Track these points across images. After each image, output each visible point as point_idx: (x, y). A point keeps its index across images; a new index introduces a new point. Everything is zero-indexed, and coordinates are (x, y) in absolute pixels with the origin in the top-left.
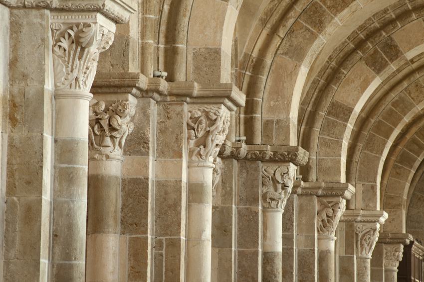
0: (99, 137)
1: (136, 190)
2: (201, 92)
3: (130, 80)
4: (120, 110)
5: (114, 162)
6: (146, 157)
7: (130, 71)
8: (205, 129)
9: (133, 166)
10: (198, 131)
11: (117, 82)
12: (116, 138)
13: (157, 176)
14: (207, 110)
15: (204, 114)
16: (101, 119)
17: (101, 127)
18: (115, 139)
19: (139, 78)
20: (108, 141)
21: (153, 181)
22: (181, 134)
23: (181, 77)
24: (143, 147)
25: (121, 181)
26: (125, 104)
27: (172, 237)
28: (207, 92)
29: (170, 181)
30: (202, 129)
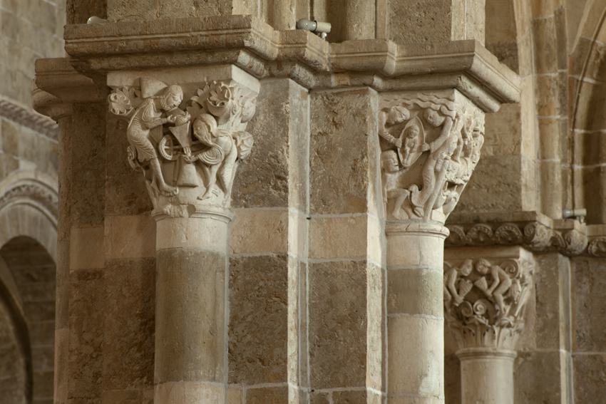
0: (172, 165)
1: (261, 284)
2: (407, 64)
3: (231, 31)
4: (215, 103)
5: (209, 221)
6: (280, 208)
7: (234, 12)
9: (252, 231)
10: (404, 152)
11: (202, 38)
12: (210, 166)
13: (313, 254)
14: (421, 104)
15: (416, 113)
16: (173, 125)
17: (175, 142)
18: (207, 169)
19: (250, 27)
20: (191, 173)
21: (303, 264)
22: (363, 157)
23: (362, 29)
24: (276, 187)
25: (227, 264)
26: (224, 88)
27: (349, 389)
28: (421, 63)
29: (341, 263)
30: (412, 148)
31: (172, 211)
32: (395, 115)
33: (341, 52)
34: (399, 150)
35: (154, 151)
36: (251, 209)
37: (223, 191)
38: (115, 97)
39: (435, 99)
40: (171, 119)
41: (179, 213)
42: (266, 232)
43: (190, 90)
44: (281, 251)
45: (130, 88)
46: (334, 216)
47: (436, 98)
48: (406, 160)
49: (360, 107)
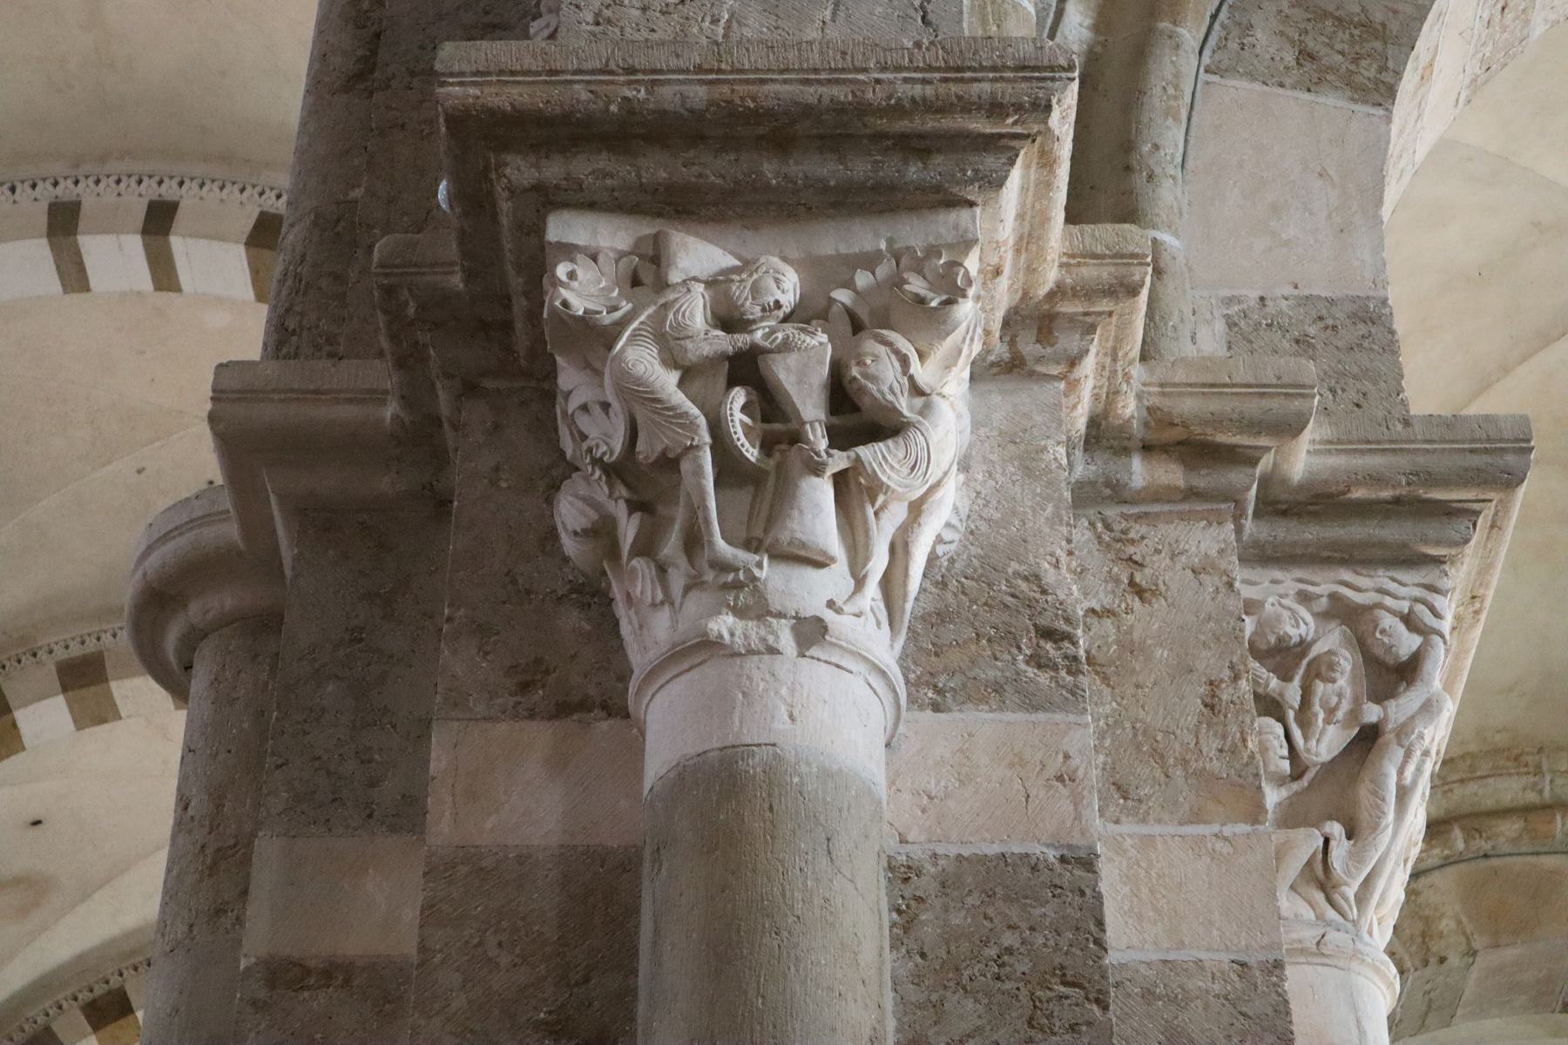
1: (1009, 939)
4: (921, 301)
8: (1354, 714)
31: (738, 632)
32: (1278, 618)
33: (1177, 380)
34: (1291, 714)
35: (702, 421)
36: (957, 715)
37: (891, 624)
38: (572, 275)
39: (1392, 586)
40: (766, 336)
41: (764, 640)
42: (1017, 785)
43: (822, 274)
44: (1077, 840)
45: (621, 255)
46: (1157, 829)
47: (1396, 585)
48: (1313, 743)
49: (1213, 552)
